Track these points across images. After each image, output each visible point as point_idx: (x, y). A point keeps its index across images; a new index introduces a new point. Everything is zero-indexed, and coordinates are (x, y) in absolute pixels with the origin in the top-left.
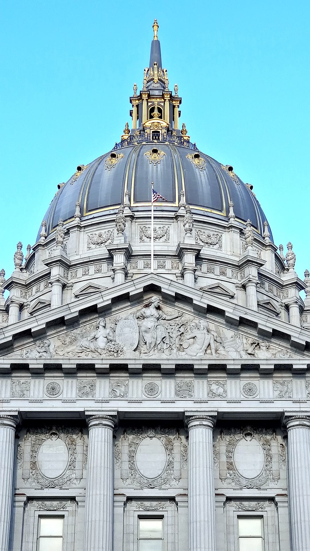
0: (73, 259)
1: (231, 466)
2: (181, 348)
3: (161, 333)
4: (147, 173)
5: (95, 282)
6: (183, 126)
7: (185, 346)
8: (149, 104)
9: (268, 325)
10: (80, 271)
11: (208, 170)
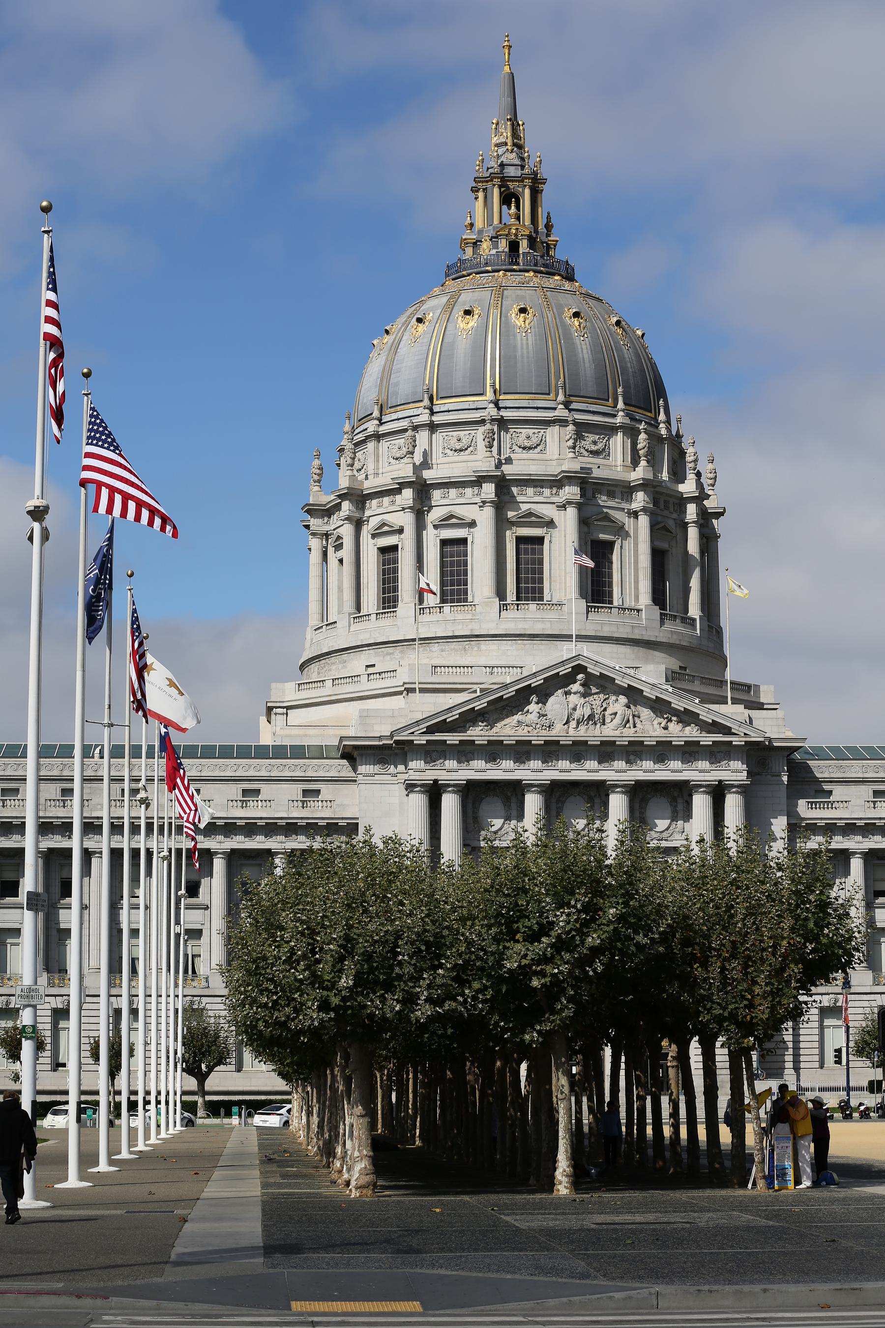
0: (427, 474)
3: (588, 712)
4: (515, 347)
5: (459, 511)
6: (549, 217)
7: (608, 720)
8: (503, 189)
9: (680, 704)
11: (592, 337)
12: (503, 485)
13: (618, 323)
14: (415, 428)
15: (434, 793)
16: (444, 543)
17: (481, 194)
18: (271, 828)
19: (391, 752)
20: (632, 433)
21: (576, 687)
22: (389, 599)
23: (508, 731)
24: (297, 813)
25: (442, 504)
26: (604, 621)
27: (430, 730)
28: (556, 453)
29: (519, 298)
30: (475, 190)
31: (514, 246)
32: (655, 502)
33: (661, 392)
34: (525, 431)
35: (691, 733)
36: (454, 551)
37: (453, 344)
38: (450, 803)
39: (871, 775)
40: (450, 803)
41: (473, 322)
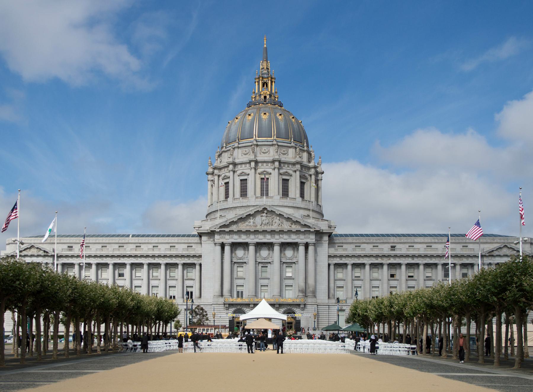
0: (237, 161)
1: (284, 254)
2: (272, 225)
3: (267, 221)
5: (245, 171)
10: (239, 166)
12: (257, 162)
13: (293, 118)
14: (234, 149)
15: (223, 246)
16: (241, 180)
17: (257, 83)
18: (177, 256)
19: (211, 234)
20: (296, 148)
21: (264, 214)
22: (227, 196)
23: (244, 228)
24: (185, 253)
25: (240, 169)
26: (286, 202)
27: (221, 227)
28: (272, 154)
29: (264, 111)
30: (255, 82)
31: (265, 97)
32: (301, 169)
33: (306, 138)
34: (264, 148)
35: (298, 228)
36: (244, 182)
37: (245, 124)
38: (227, 249)
39: (354, 241)
40: (227, 249)
41: (250, 118)
